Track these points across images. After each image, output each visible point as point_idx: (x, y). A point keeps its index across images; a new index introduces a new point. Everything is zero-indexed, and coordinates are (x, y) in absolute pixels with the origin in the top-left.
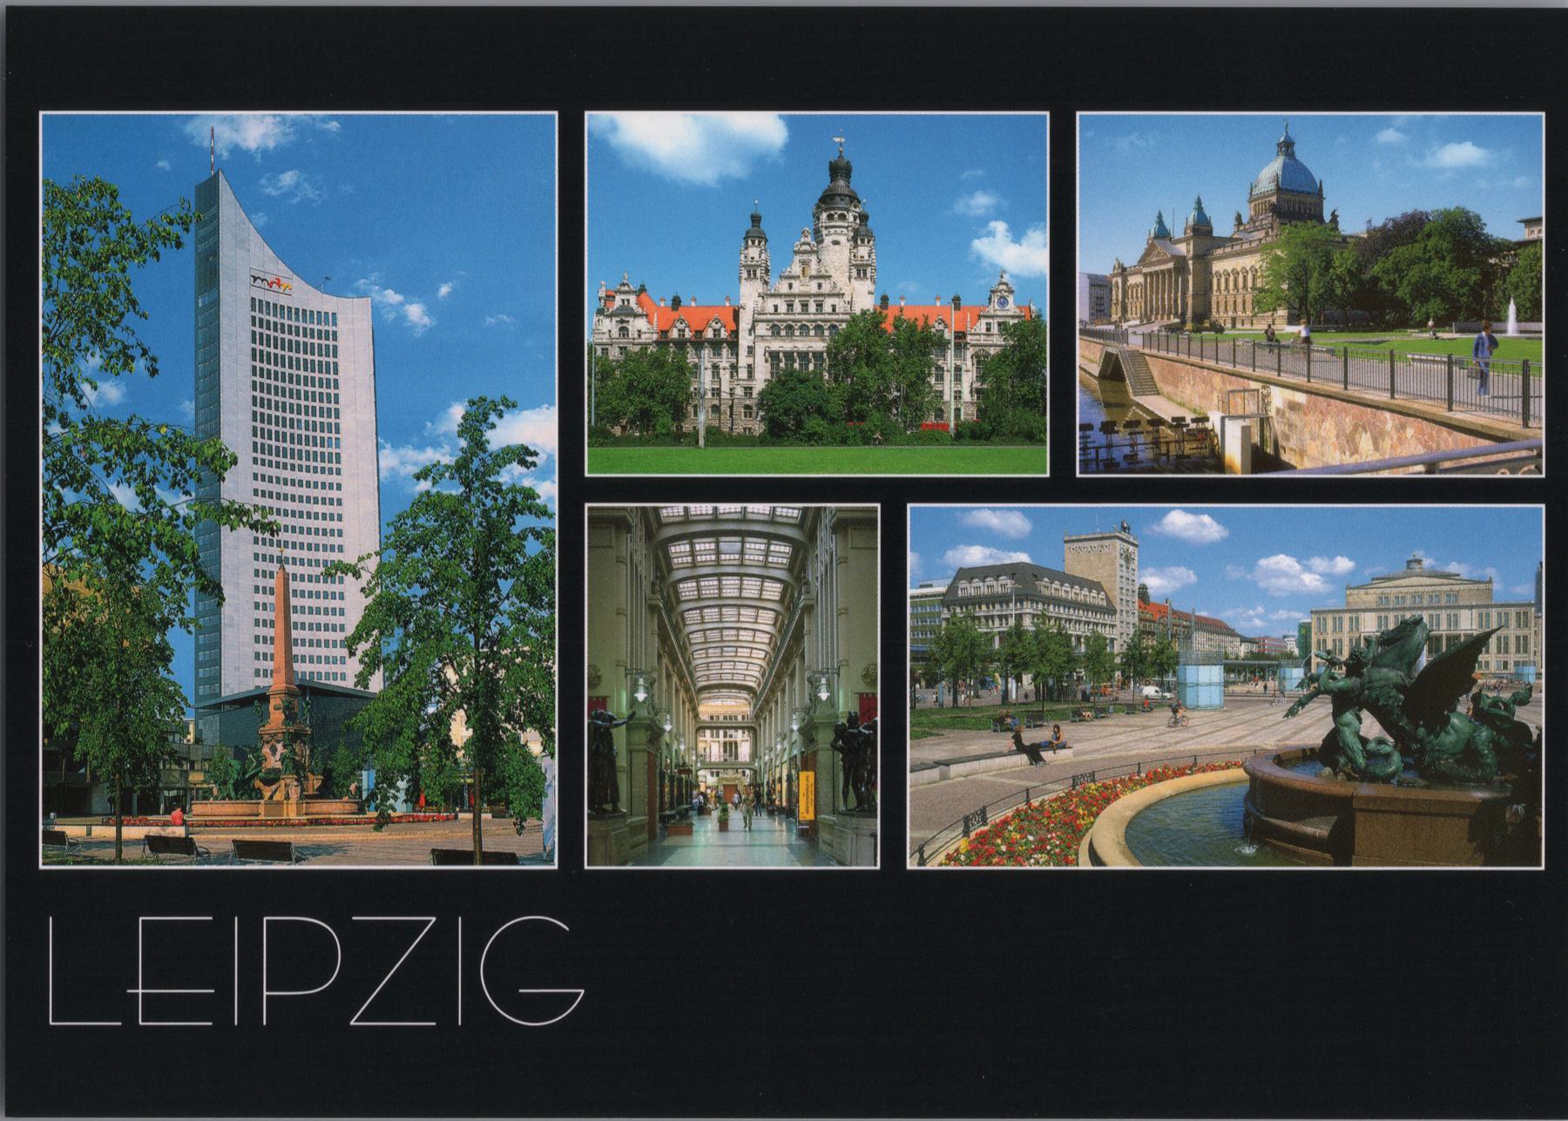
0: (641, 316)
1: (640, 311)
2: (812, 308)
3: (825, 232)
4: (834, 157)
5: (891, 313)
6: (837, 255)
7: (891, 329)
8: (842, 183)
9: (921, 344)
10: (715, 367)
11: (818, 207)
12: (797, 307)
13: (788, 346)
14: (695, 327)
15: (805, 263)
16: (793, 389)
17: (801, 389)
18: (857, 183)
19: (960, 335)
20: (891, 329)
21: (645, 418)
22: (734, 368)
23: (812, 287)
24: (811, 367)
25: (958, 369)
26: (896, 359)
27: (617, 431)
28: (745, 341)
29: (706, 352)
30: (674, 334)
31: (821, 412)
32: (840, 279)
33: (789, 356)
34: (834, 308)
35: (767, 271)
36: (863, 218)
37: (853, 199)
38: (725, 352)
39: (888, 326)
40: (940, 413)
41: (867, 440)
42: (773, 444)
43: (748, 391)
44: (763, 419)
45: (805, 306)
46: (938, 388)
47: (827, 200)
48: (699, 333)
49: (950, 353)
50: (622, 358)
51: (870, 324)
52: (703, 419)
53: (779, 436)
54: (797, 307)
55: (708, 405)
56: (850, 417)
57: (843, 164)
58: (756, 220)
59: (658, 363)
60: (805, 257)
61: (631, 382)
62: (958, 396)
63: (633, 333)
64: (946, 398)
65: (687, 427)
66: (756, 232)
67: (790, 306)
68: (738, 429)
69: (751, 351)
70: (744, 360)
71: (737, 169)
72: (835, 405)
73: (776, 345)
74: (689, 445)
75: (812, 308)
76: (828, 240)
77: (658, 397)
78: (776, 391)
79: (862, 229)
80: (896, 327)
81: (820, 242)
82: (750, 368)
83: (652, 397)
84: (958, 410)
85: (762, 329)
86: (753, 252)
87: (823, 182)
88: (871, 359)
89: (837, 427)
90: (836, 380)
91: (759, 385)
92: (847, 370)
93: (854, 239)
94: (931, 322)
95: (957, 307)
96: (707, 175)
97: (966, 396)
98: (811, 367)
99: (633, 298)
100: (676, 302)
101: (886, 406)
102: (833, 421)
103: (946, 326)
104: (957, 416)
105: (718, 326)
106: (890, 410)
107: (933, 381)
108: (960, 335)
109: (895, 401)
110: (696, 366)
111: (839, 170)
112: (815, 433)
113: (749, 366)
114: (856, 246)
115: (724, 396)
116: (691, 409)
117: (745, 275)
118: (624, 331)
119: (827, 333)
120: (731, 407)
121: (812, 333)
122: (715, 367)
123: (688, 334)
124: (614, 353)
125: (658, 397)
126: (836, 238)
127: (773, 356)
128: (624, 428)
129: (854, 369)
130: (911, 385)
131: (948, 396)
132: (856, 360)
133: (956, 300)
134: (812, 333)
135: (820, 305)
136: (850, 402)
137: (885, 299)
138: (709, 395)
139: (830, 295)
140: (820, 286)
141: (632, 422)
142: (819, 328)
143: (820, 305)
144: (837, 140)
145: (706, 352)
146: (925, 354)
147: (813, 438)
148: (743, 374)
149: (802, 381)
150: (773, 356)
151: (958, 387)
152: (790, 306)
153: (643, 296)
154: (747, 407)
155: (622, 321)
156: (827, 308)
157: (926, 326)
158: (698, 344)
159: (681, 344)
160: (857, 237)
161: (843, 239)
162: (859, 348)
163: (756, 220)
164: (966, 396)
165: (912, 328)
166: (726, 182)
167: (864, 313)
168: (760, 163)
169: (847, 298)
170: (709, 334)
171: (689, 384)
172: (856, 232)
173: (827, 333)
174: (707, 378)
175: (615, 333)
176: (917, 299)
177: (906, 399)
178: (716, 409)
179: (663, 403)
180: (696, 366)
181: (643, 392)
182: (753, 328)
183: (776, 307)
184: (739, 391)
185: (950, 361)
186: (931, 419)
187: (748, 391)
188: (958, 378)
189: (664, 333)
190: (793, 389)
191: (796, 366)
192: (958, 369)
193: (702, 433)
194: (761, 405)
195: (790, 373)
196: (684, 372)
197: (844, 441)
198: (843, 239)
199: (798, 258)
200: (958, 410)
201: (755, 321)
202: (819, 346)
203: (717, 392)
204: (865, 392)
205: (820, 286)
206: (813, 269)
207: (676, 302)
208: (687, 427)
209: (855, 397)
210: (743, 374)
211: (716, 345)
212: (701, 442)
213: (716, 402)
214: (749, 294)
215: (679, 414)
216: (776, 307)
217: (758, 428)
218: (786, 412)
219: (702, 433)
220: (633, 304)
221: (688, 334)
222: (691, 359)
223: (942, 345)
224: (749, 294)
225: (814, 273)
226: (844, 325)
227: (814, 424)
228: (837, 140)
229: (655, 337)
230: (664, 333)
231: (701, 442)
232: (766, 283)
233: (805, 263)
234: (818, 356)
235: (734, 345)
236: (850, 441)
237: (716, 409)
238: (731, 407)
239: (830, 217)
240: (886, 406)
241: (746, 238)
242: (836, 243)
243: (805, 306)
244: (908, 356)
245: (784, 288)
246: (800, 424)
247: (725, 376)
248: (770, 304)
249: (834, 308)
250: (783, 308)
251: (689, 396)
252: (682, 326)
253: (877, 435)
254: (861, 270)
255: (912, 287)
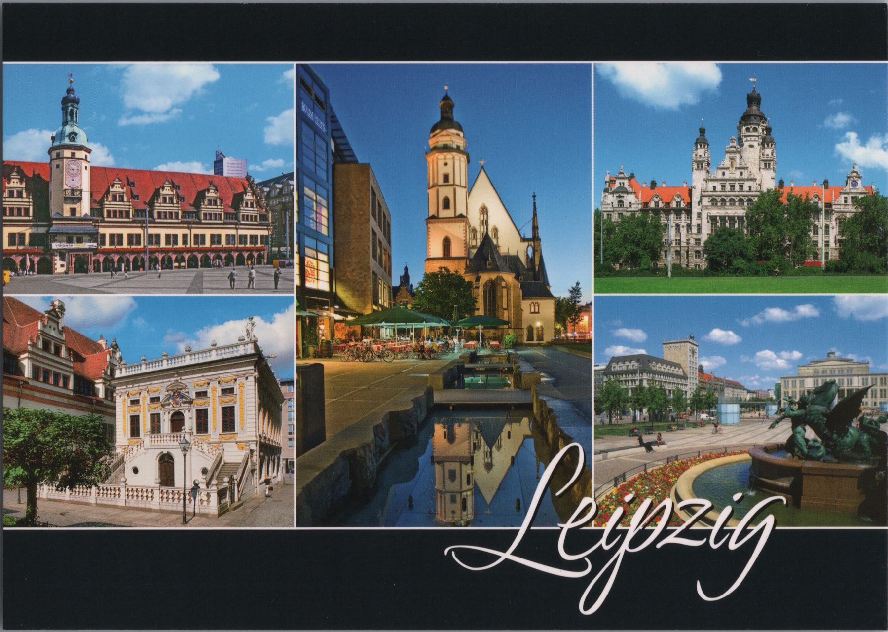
0: (631, 193)
1: (630, 190)
2: (737, 188)
3: (744, 139)
4: (750, 91)
5: (785, 191)
6: (752, 154)
7: (786, 202)
8: (754, 107)
9: (804, 211)
10: (678, 226)
11: (740, 123)
12: (728, 188)
13: (722, 212)
14: (665, 200)
15: (732, 159)
16: (725, 240)
17: (731, 240)
18: (764, 108)
19: (829, 205)
20: (786, 202)
21: (634, 259)
22: (689, 226)
23: (737, 175)
24: (736, 226)
25: (827, 227)
26: (789, 220)
27: (617, 267)
28: (695, 209)
29: (672, 216)
30: (652, 205)
31: (743, 255)
32: (754, 169)
33: (723, 218)
34: (750, 187)
35: (709, 164)
36: (768, 130)
37: (762, 118)
38: (683, 216)
39: (784, 200)
40: (816, 255)
41: (771, 273)
42: (713, 275)
43: (698, 241)
44: (707, 259)
45: (732, 187)
46: (815, 239)
47: (746, 119)
48: (668, 204)
49: (822, 216)
50: (619, 220)
51: (773, 197)
52: (669, 260)
53: (717, 270)
54: (728, 188)
55: (673, 250)
56: (760, 258)
57: (756, 95)
58: (702, 131)
59: (642, 224)
60: (732, 155)
61: (625, 236)
62: (827, 244)
63: (626, 204)
64: (820, 245)
65: (660, 264)
66: (702, 140)
67: (723, 186)
68: (692, 266)
69: (699, 215)
70: (695, 221)
71: (691, 99)
72: (751, 251)
73: (714, 212)
74: (662, 276)
75: (737, 188)
76: (746, 144)
77: (642, 246)
78: (714, 241)
79: (768, 137)
80: (789, 200)
81: (741, 145)
82: (699, 227)
83: (638, 245)
84: (827, 253)
85: (706, 201)
86: (701, 152)
87: (744, 107)
88: (773, 221)
89: (753, 264)
90: (751, 234)
91: (704, 237)
92: (758, 228)
93: (763, 144)
94: (811, 197)
95: (827, 187)
96: (671, 102)
97: (832, 245)
98: (736, 226)
99: (626, 182)
100: (653, 184)
101: (783, 251)
102: (750, 260)
103: (820, 199)
104: (827, 257)
105: (679, 200)
106: (785, 254)
107: (811, 235)
108: (829, 205)
109: (788, 248)
110: (666, 225)
111: (753, 99)
112: (738, 269)
113: (698, 225)
114: (763, 148)
115: (683, 244)
116: (663, 253)
117: (695, 166)
118: (621, 203)
119: (746, 204)
120: (687, 252)
121: (737, 204)
122: (678, 226)
123: (661, 205)
124: (615, 217)
125: (642, 246)
126: (751, 143)
127: (713, 219)
128: (621, 265)
129: (763, 227)
130: (798, 238)
131: (821, 245)
132: (764, 222)
133: (826, 182)
134: (737, 204)
135: (741, 186)
136: (760, 249)
137: (781, 183)
138: (674, 244)
139: (748, 180)
140: (742, 173)
141: (626, 261)
142: (741, 201)
143: (741, 186)
144: (752, 80)
145: (672, 216)
146: (807, 217)
147: (737, 272)
148: (694, 230)
149: (731, 235)
150: (713, 219)
151: (827, 238)
152: (723, 186)
153: (633, 180)
154: (697, 252)
155: (620, 197)
156: (746, 188)
157: (807, 200)
158: (667, 211)
159: (656, 211)
160: (764, 143)
161: (755, 144)
162: (766, 214)
163: (702, 131)
164: (832, 245)
165: (798, 201)
166: (682, 107)
167: (769, 191)
168: (705, 95)
169: (758, 182)
170: (674, 205)
171: (661, 237)
172: (764, 139)
173: (746, 204)
174: (672, 232)
175: (616, 204)
176: (802, 182)
177: (795, 246)
178: (678, 253)
179: (645, 249)
180: (666, 225)
181: (633, 242)
182: (700, 202)
183: (714, 187)
184: (692, 242)
185: (822, 221)
186: (811, 259)
187: (698, 241)
188: (827, 232)
189: (646, 204)
190: (725, 240)
191: (727, 225)
192: (827, 227)
193: (670, 269)
194: (705, 251)
195: (724, 230)
196: (660, 229)
197: (757, 273)
198: (755, 144)
199: (728, 156)
200: (827, 253)
201: (702, 196)
202: (741, 212)
203: (679, 242)
204: (770, 242)
205: (742, 173)
206: (738, 162)
207: (653, 184)
208: (660, 264)
209: (764, 244)
210: (694, 230)
211: (678, 212)
212: (669, 274)
213: (678, 249)
214: (698, 179)
215: (655, 256)
216: (714, 187)
217: (704, 265)
218: (721, 255)
219: (670, 269)
220: (626, 186)
221: (661, 205)
222: (663, 221)
223: (818, 211)
224: (698, 179)
225: (738, 166)
226: (756, 199)
227: (739, 262)
228: (752, 80)
229: (640, 206)
230: (646, 204)
231: (669, 274)
232: (708, 172)
233: (732, 159)
234: (740, 218)
235: (689, 212)
236: (761, 273)
237: (678, 253)
238: (687, 252)
239: (748, 130)
240: (783, 251)
241: (696, 144)
242: (751, 146)
243: (732, 187)
244: (796, 218)
245: (720, 176)
246: (729, 263)
247: (683, 231)
248: (711, 185)
249: (750, 187)
250: (719, 188)
251: (661, 245)
252: (657, 200)
253: (777, 270)
254: (767, 164)
255: (798, 174)
